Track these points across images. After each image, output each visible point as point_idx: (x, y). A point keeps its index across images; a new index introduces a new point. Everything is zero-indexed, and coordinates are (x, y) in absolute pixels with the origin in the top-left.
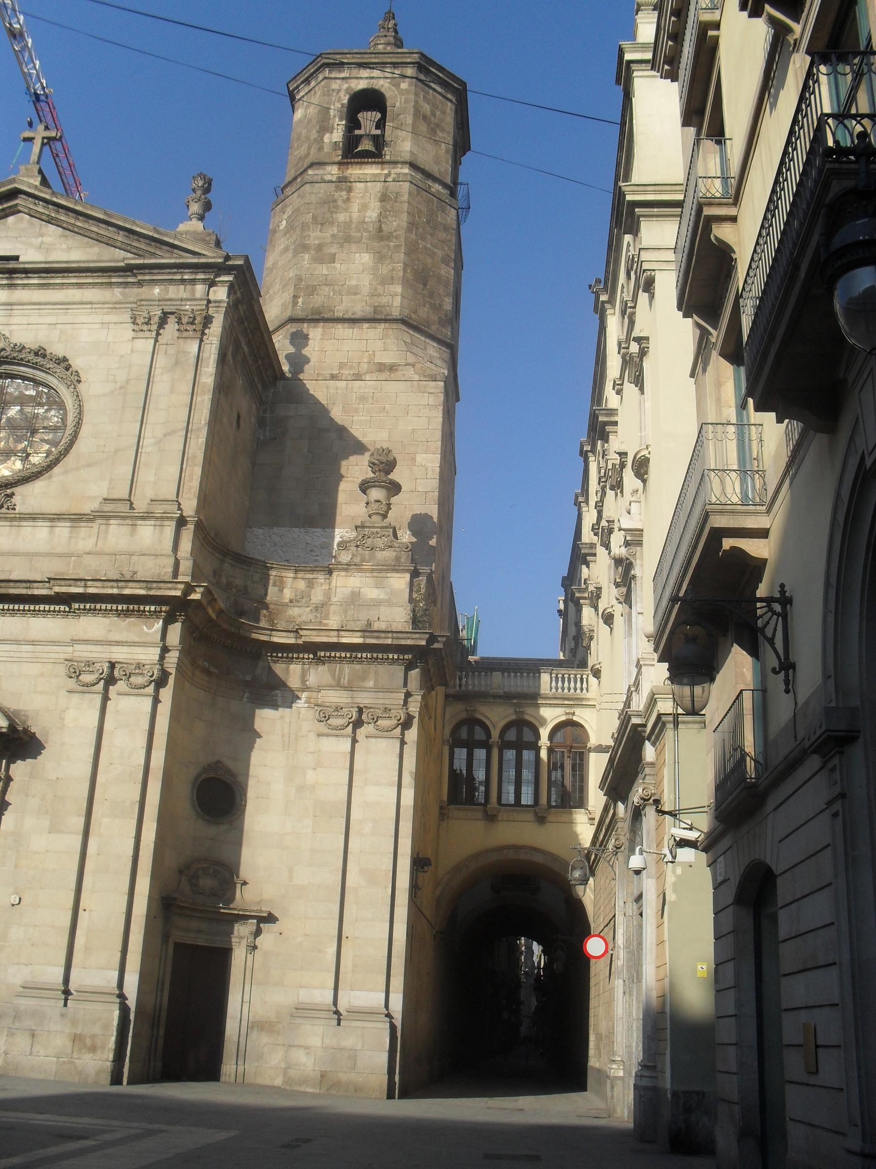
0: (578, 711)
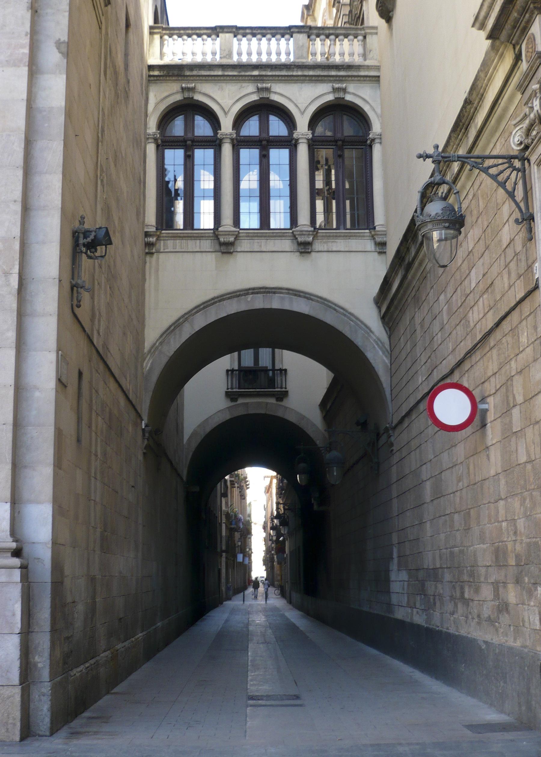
0: (351, 87)
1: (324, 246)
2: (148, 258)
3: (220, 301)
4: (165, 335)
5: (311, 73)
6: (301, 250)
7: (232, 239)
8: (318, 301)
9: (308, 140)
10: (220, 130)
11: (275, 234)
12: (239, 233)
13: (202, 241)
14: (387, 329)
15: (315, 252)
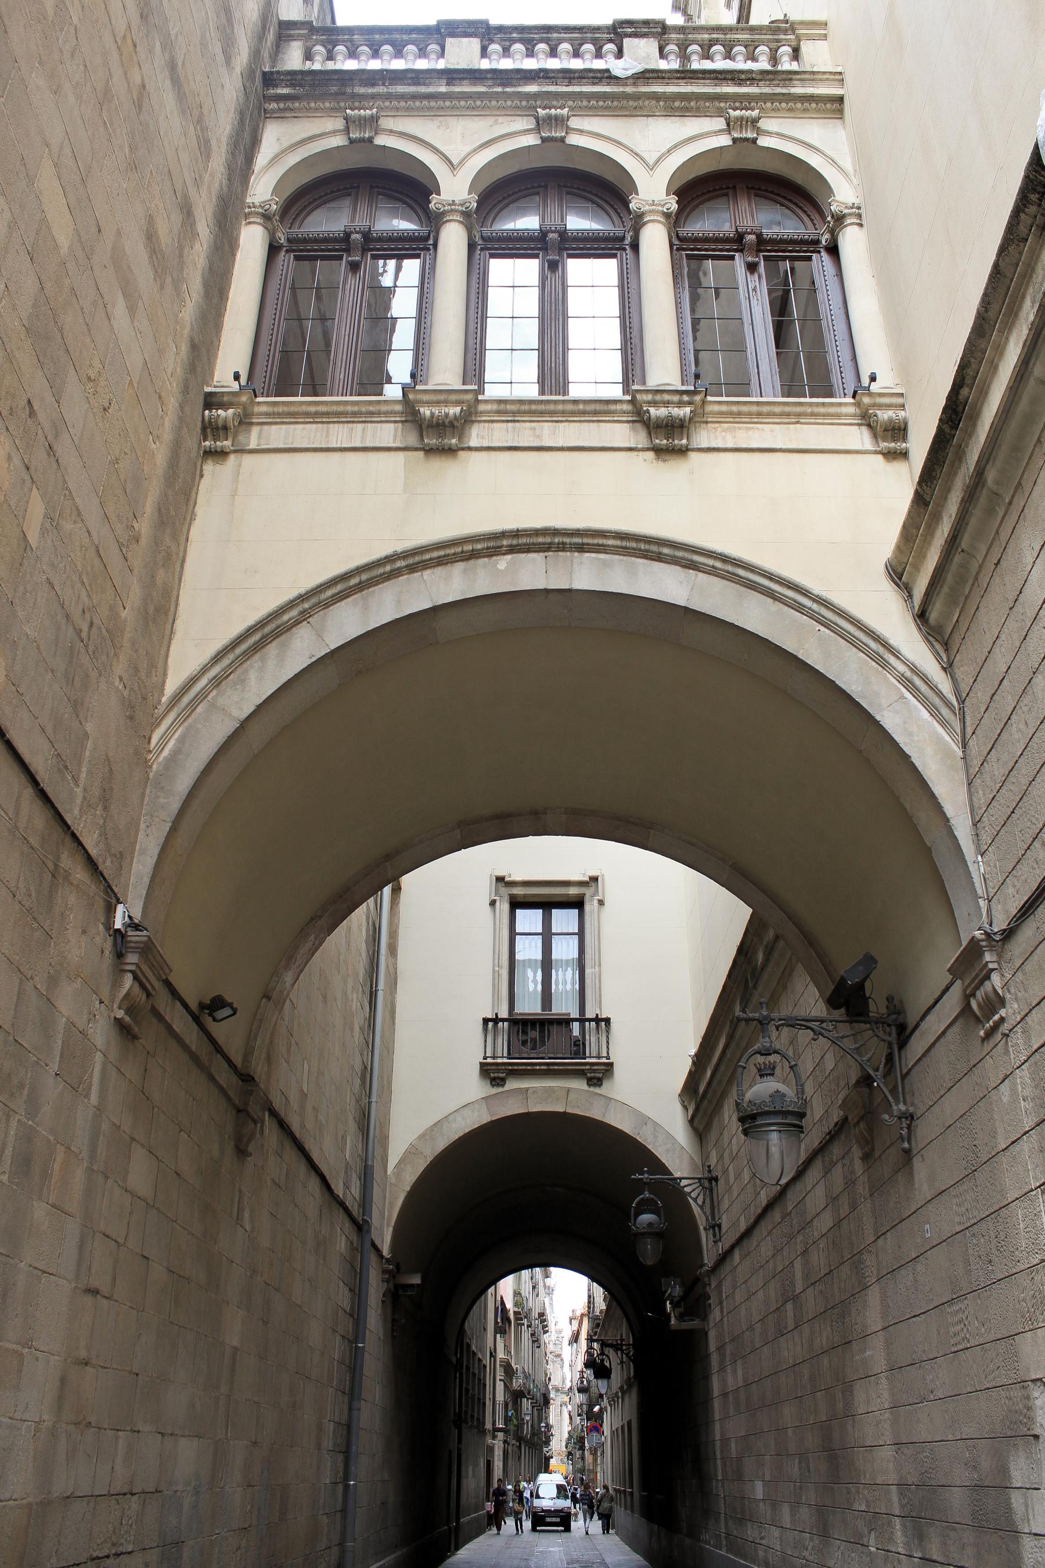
1: (724, 438)
2: (209, 467)
3: (412, 569)
4: (231, 657)
8: (713, 572)
13: (369, 425)
14: (938, 646)
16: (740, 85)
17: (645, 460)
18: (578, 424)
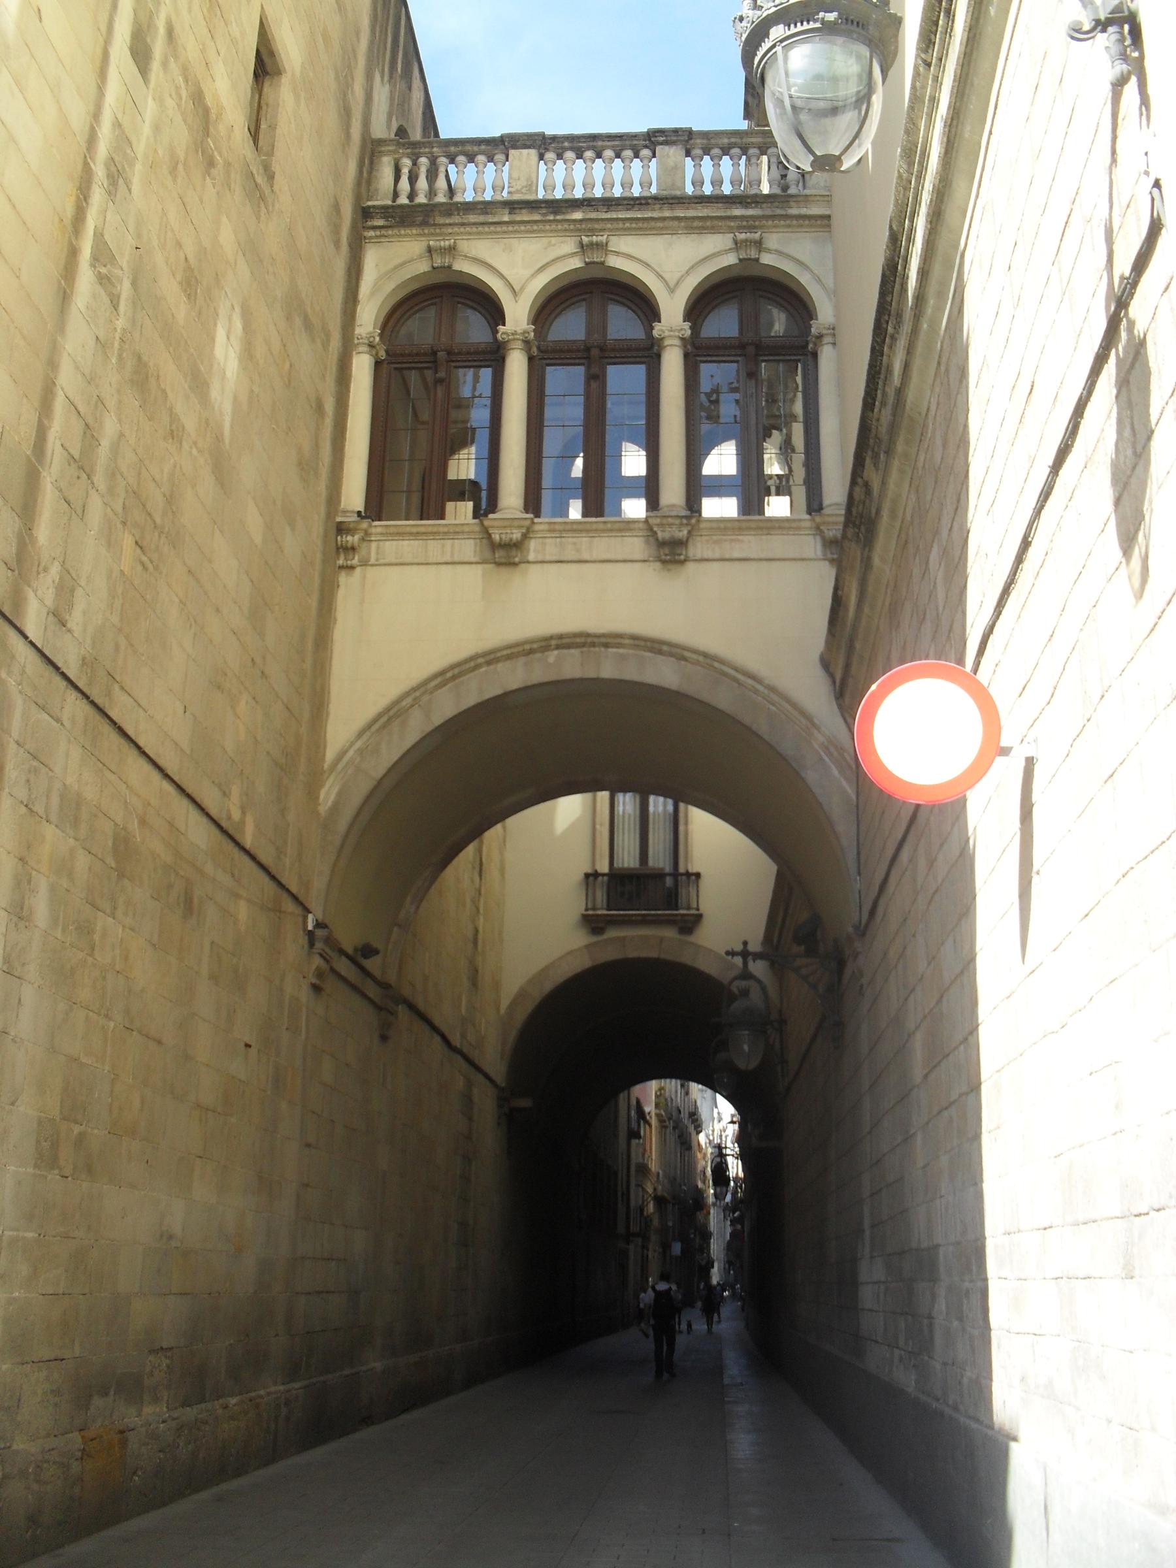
0: (773, 240)
2: (343, 578)
5: (691, 213)
6: (663, 557)
7: (516, 535)
8: (697, 663)
9: (682, 339)
10: (504, 325)
11: (609, 526)
12: (533, 523)
13: (456, 541)
15: (696, 560)
16: (746, 207)
17: (654, 570)
18: (607, 539)
